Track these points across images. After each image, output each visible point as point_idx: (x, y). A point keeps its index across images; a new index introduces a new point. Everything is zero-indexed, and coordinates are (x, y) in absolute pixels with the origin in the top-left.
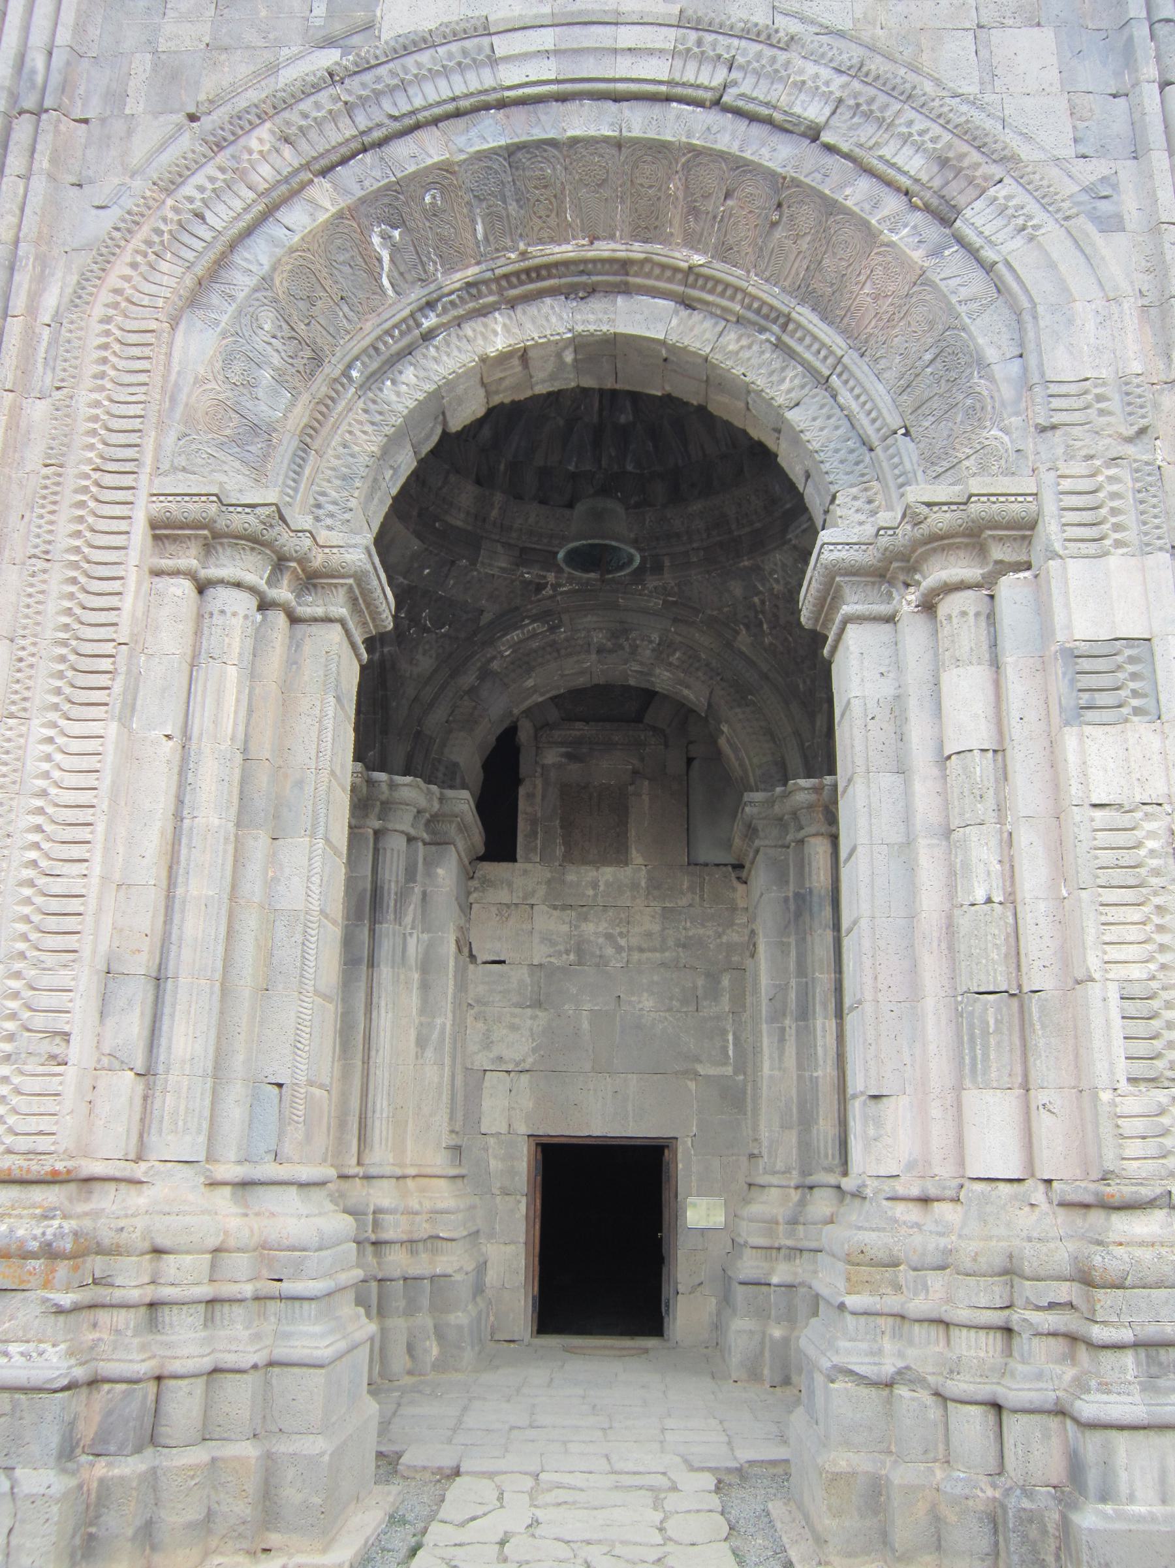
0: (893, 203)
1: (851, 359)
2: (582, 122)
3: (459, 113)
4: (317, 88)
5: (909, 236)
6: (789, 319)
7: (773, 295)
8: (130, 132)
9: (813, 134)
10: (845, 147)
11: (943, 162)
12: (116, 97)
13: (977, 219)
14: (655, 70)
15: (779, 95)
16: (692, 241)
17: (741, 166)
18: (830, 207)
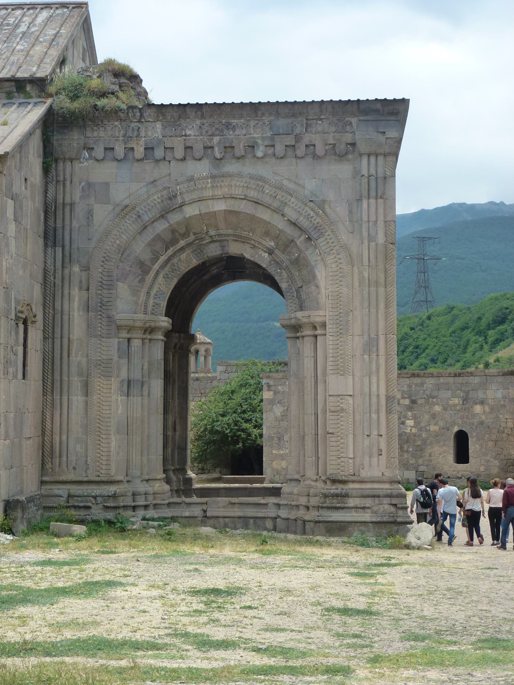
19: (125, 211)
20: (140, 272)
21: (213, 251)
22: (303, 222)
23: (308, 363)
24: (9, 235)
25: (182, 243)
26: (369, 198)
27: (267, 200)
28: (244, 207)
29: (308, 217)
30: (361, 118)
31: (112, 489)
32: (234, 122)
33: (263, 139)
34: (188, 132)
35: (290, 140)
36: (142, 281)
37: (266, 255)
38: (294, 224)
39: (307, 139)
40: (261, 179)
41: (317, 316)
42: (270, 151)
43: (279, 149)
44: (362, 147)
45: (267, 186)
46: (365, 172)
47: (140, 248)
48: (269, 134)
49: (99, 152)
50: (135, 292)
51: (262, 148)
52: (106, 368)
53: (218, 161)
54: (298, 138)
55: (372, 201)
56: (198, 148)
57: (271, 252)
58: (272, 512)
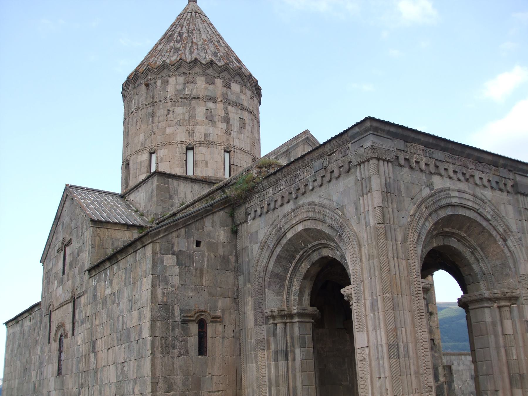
0: (498, 237)
1: (485, 259)
2: (461, 212)
3: (446, 206)
4: (430, 197)
5: (501, 242)
6: (476, 249)
7: (475, 244)
8: (404, 200)
9: (488, 220)
10: (493, 225)
11: (505, 231)
12: (400, 191)
13: (509, 242)
14: (470, 204)
15: (485, 213)
16: (465, 232)
17: (479, 224)
18: (491, 235)
19: (264, 245)
20: (279, 281)
21: (315, 257)
24: (168, 274)
25: (298, 257)
26: (363, 195)
27: (318, 216)
28: (310, 225)
29: (336, 220)
30: (352, 142)
34: (282, 188)
35: (322, 173)
36: (283, 286)
37: (338, 252)
38: (331, 227)
40: (313, 203)
42: (316, 184)
44: (355, 161)
45: (316, 207)
46: (359, 178)
50: (279, 294)
51: (311, 184)
55: (365, 196)
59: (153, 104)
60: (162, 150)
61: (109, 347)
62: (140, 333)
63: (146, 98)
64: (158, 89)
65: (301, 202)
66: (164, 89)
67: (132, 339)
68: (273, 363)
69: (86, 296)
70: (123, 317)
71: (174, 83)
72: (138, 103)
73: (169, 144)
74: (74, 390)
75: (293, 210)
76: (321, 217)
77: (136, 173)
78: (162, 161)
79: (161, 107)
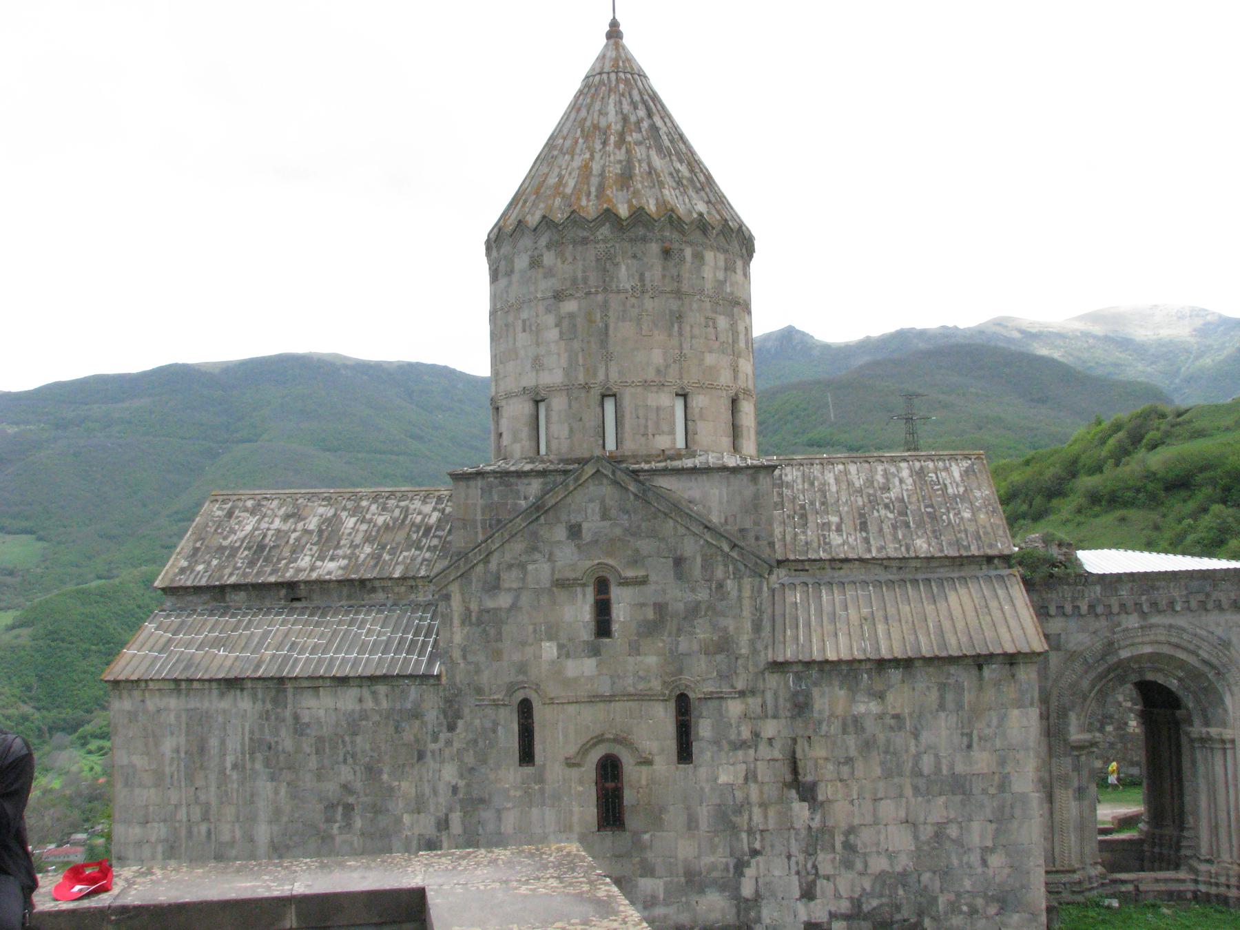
22: (1214, 661)
23: (1219, 770)
27: (1185, 644)
28: (1166, 650)
31: (1076, 877)
32: (1158, 584)
33: (1181, 596)
35: (1201, 597)
38: (1205, 662)
39: (1215, 595)
41: (1228, 734)
43: (1193, 604)
47: (1085, 684)
48: (1184, 593)
49: (1052, 610)
50: (1078, 716)
52: (1065, 780)
53: (1143, 615)
54: (1208, 595)
56: (1130, 604)
57: (1180, 679)
58: (1192, 887)
59: (678, 294)
60: (701, 397)
61: (879, 796)
62: (1003, 786)
63: (664, 276)
64: (688, 265)
65: (1154, 620)
66: (699, 269)
67: (974, 791)
68: (1073, 804)
69: (754, 703)
70: (937, 756)
71: (712, 264)
72: (642, 278)
73: (712, 387)
74: (707, 860)
75: (1142, 627)
76: (1192, 647)
77: (646, 427)
78: (702, 417)
79: (695, 306)
